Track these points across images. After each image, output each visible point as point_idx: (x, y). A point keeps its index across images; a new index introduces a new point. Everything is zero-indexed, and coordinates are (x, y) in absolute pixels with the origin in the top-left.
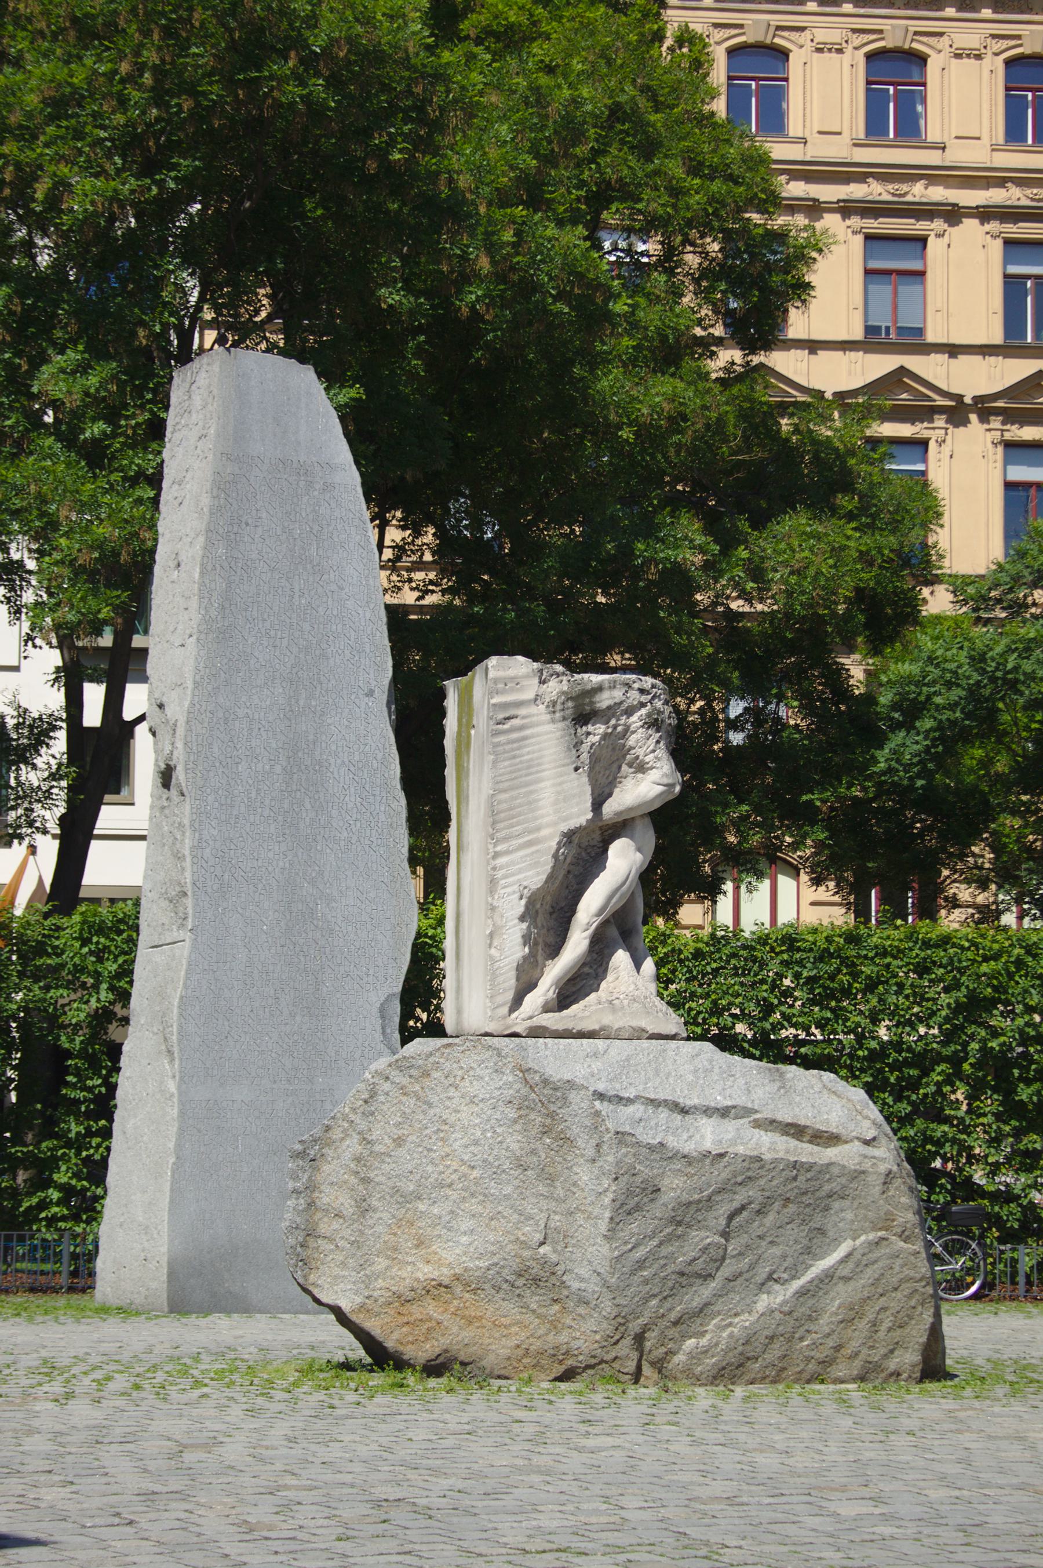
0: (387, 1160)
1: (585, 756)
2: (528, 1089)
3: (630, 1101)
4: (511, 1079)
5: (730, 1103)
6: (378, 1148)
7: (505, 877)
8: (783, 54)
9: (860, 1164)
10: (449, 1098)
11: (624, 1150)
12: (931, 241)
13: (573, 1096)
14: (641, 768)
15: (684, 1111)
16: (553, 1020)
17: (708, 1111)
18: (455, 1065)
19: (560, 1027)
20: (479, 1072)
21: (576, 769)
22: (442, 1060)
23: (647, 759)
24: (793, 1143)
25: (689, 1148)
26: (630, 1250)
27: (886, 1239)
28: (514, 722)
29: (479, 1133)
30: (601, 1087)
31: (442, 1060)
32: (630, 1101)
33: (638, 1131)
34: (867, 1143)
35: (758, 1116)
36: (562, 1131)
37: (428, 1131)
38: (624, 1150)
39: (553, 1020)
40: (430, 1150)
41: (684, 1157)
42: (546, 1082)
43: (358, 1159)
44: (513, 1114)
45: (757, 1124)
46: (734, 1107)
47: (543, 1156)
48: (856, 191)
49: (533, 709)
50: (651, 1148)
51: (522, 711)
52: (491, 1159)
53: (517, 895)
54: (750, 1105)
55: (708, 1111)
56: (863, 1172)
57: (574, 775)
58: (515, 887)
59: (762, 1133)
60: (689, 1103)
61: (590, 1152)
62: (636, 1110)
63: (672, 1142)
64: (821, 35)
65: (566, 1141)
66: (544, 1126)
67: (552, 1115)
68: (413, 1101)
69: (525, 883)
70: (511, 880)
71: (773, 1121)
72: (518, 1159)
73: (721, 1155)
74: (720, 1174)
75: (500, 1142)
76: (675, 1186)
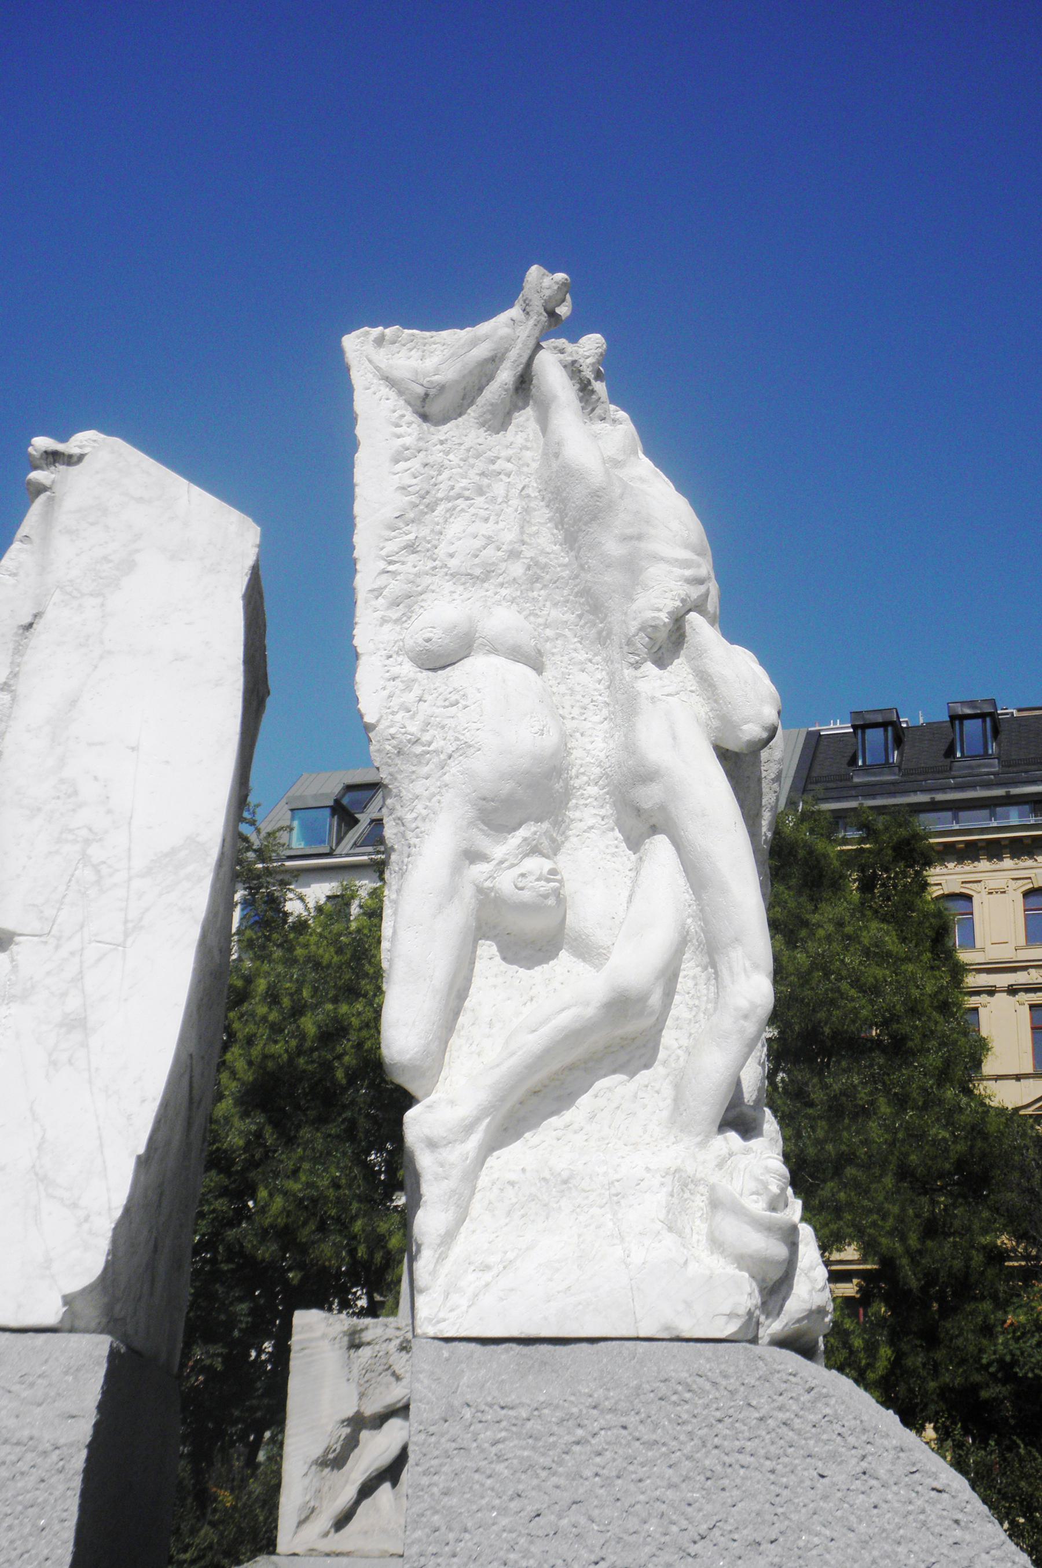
1: (355, 1372)
8: (969, 898)
12: (981, 1010)
28: (306, 1351)
39: (325, 1545)
48: (1020, 978)
64: (992, 885)
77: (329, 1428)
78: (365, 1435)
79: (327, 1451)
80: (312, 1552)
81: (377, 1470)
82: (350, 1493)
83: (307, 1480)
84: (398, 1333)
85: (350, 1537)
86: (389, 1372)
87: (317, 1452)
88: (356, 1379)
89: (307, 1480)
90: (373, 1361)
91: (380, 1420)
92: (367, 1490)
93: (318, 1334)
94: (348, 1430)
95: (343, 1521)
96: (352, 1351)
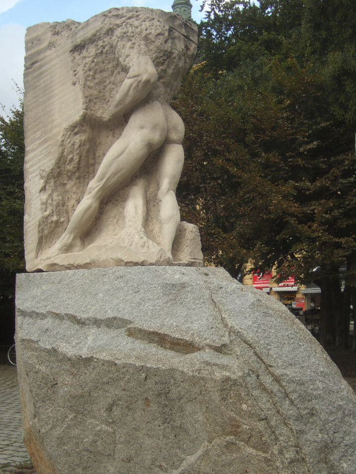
1: (81, 73)
3: (43, 316)
7: (32, 166)
9: (199, 371)
11: (29, 354)
17: (97, 323)
19: (66, 263)
21: (74, 84)
24: (153, 349)
26: (51, 429)
27: (232, 443)
28: (37, 65)
32: (43, 316)
34: (220, 349)
35: (131, 326)
38: (29, 354)
39: (62, 259)
41: (69, 360)
45: (131, 333)
49: (49, 52)
51: (42, 56)
55: (97, 323)
56: (203, 379)
57: (73, 87)
60: (84, 316)
62: (48, 323)
69: (43, 168)
70: (34, 168)
71: (140, 331)
73: (89, 360)
74: (89, 376)
76: (67, 385)
77: (60, 138)
78: (104, 138)
79: (61, 161)
80: (53, 267)
81: (114, 174)
82: (87, 201)
83: (44, 196)
84: (118, 22)
86: (119, 69)
87: (48, 164)
88: (82, 82)
89: (44, 196)
90: (100, 59)
91: (121, 120)
92: (112, 197)
93: (45, 44)
94: (83, 137)
95: (88, 231)
96: (76, 54)
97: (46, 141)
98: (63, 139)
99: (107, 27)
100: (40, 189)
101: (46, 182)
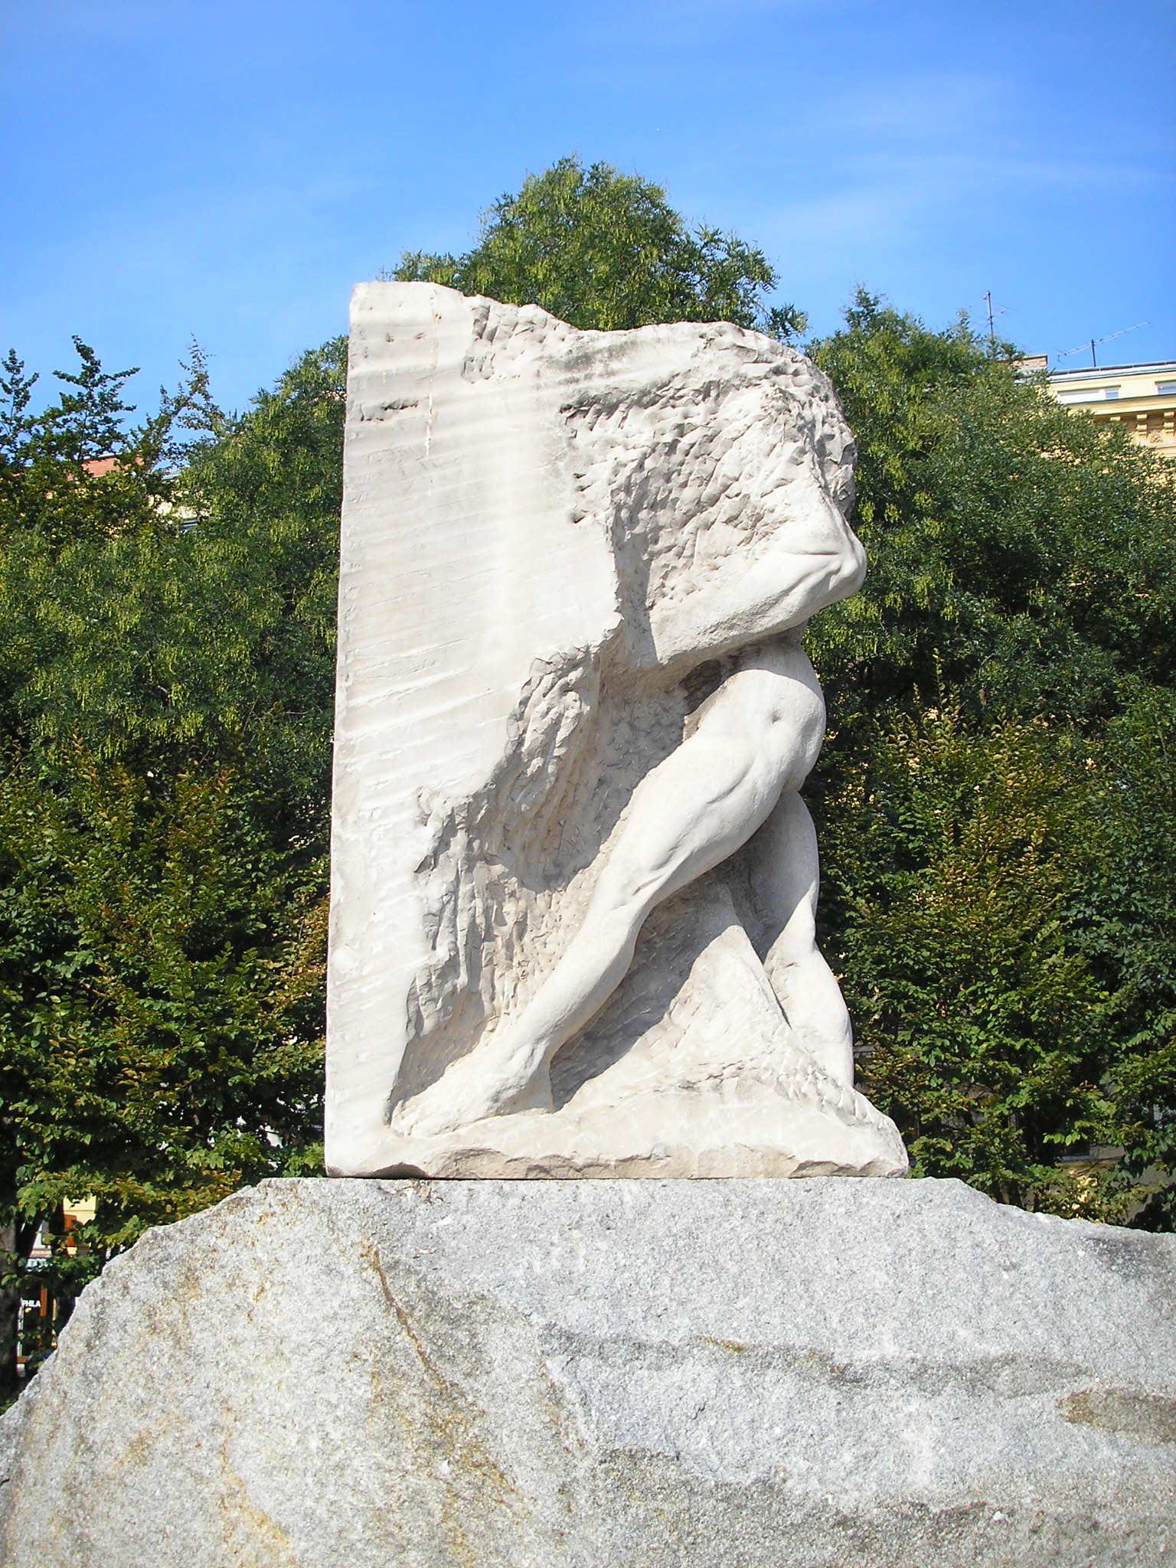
0: (120, 1495)
2: (393, 1320)
4: (355, 1293)
5: (995, 1351)
6: (105, 1464)
10: (235, 1342)
11: (639, 1509)
13: (497, 1344)
14: (754, 524)
15: (845, 1378)
16: (534, 1133)
17: (922, 1377)
18: (246, 1256)
20: (291, 1272)
22: (222, 1243)
23: (769, 502)
25: (856, 1495)
29: (293, 1439)
30: (574, 1315)
31: (222, 1243)
32: (671, 1354)
33: (698, 1441)
35: (1083, 1384)
36: (474, 1447)
37: (194, 1428)
38: (639, 1509)
40: (199, 1478)
41: (843, 1523)
42: (431, 1299)
43: (70, 1490)
44: (364, 1391)
45: (1081, 1410)
46: (1009, 1360)
47: (439, 1516)
50: (732, 1498)
51: (434, 392)
52: (322, 1512)
53: (413, 813)
54: (1057, 1352)
58: (407, 794)
59: (1100, 1436)
60: (863, 1356)
61: (549, 1510)
62: (695, 1377)
63: (804, 1481)
65: (485, 1467)
66: (434, 1426)
67: (447, 1393)
68: (167, 1345)
71: (1131, 1400)
72: (380, 1515)
73: (961, 1516)
75: (340, 1467)
85: (619, 1101)
89: (436, 885)
95: (583, 1047)
97: (446, 687)
98: (526, 694)
99: (710, 374)
100: (420, 859)
101: (443, 842)
